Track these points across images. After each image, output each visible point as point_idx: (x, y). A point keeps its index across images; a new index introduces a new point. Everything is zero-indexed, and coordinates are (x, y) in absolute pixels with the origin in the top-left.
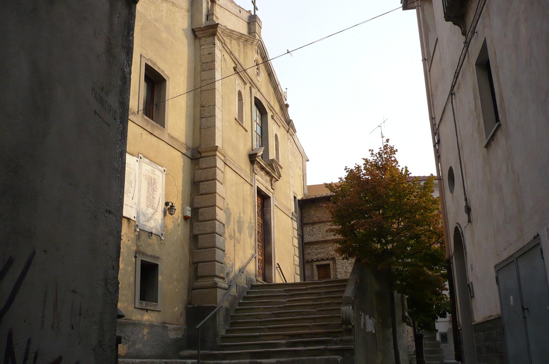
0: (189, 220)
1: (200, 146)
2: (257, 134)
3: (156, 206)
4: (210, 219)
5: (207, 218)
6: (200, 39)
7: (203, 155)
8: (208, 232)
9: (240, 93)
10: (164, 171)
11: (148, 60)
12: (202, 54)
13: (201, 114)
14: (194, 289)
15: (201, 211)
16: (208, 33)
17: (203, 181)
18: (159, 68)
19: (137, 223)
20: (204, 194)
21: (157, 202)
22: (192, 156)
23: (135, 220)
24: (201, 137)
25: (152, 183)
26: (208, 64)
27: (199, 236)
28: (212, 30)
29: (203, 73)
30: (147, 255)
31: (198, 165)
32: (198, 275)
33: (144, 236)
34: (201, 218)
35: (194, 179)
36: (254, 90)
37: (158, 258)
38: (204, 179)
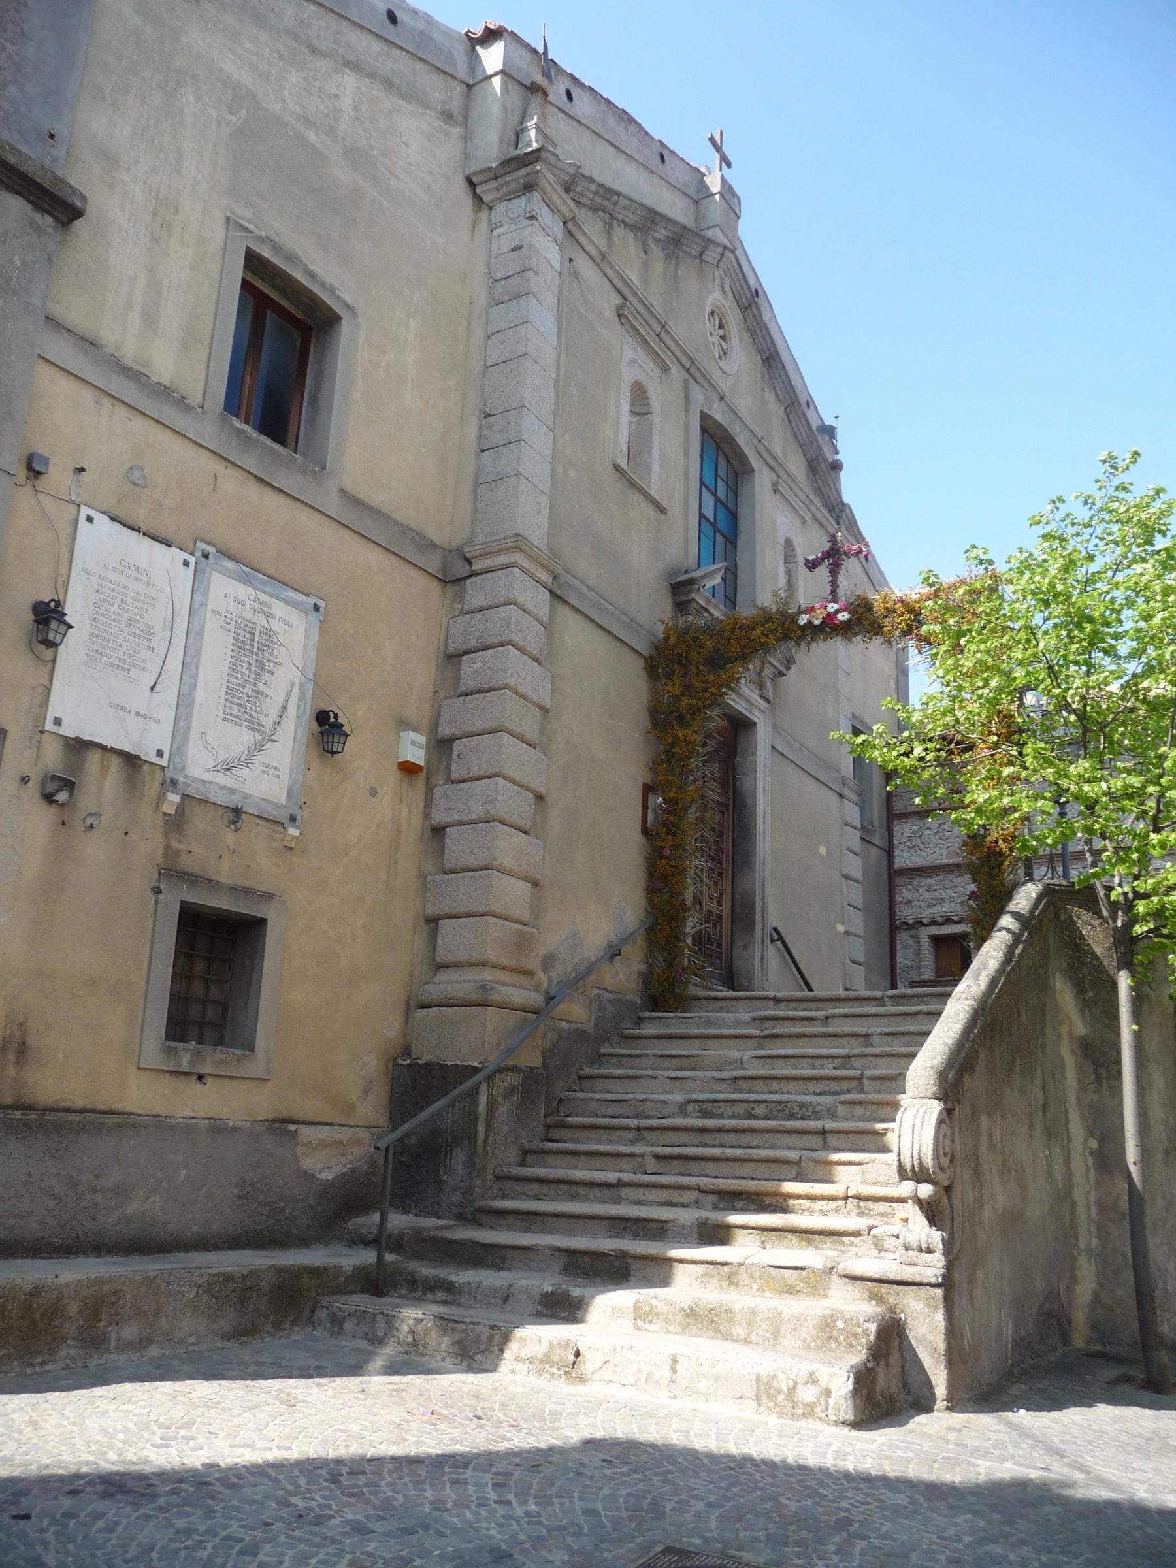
0: (422, 776)
1: (470, 540)
2: (716, 530)
3: (268, 722)
4: (482, 773)
5: (475, 772)
6: (490, 208)
7: (478, 565)
8: (474, 816)
9: (639, 393)
10: (317, 608)
11: (262, 240)
12: (494, 253)
13: (480, 438)
14: (422, 1007)
15: (458, 746)
16: (513, 185)
17: (469, 652)
18: (312, 276)
19: (169, 774)
20: (472, 693)
21: (273, 711)
22: (445, 571)
23: (164, 762)
24: (475, 510)
25: (254, 647)
26: (511, 280)
27: (449, 830)
28: (524, 171)
29: (496, 312)
30: (213, 885)
31: (462, 601)
32: (438, 959)
33: (200, 822)
34: (457, 771)
35: (446, 644)
36: (698, 395)
37: (268, 896)
38: (472, 643)
